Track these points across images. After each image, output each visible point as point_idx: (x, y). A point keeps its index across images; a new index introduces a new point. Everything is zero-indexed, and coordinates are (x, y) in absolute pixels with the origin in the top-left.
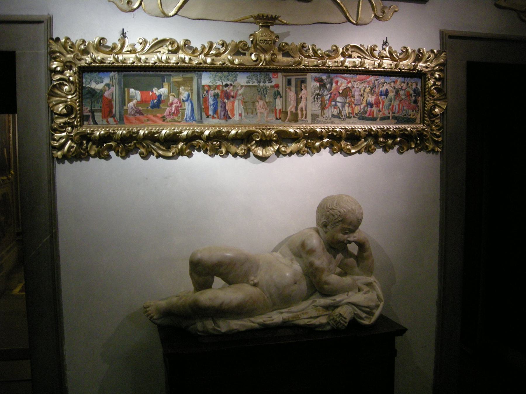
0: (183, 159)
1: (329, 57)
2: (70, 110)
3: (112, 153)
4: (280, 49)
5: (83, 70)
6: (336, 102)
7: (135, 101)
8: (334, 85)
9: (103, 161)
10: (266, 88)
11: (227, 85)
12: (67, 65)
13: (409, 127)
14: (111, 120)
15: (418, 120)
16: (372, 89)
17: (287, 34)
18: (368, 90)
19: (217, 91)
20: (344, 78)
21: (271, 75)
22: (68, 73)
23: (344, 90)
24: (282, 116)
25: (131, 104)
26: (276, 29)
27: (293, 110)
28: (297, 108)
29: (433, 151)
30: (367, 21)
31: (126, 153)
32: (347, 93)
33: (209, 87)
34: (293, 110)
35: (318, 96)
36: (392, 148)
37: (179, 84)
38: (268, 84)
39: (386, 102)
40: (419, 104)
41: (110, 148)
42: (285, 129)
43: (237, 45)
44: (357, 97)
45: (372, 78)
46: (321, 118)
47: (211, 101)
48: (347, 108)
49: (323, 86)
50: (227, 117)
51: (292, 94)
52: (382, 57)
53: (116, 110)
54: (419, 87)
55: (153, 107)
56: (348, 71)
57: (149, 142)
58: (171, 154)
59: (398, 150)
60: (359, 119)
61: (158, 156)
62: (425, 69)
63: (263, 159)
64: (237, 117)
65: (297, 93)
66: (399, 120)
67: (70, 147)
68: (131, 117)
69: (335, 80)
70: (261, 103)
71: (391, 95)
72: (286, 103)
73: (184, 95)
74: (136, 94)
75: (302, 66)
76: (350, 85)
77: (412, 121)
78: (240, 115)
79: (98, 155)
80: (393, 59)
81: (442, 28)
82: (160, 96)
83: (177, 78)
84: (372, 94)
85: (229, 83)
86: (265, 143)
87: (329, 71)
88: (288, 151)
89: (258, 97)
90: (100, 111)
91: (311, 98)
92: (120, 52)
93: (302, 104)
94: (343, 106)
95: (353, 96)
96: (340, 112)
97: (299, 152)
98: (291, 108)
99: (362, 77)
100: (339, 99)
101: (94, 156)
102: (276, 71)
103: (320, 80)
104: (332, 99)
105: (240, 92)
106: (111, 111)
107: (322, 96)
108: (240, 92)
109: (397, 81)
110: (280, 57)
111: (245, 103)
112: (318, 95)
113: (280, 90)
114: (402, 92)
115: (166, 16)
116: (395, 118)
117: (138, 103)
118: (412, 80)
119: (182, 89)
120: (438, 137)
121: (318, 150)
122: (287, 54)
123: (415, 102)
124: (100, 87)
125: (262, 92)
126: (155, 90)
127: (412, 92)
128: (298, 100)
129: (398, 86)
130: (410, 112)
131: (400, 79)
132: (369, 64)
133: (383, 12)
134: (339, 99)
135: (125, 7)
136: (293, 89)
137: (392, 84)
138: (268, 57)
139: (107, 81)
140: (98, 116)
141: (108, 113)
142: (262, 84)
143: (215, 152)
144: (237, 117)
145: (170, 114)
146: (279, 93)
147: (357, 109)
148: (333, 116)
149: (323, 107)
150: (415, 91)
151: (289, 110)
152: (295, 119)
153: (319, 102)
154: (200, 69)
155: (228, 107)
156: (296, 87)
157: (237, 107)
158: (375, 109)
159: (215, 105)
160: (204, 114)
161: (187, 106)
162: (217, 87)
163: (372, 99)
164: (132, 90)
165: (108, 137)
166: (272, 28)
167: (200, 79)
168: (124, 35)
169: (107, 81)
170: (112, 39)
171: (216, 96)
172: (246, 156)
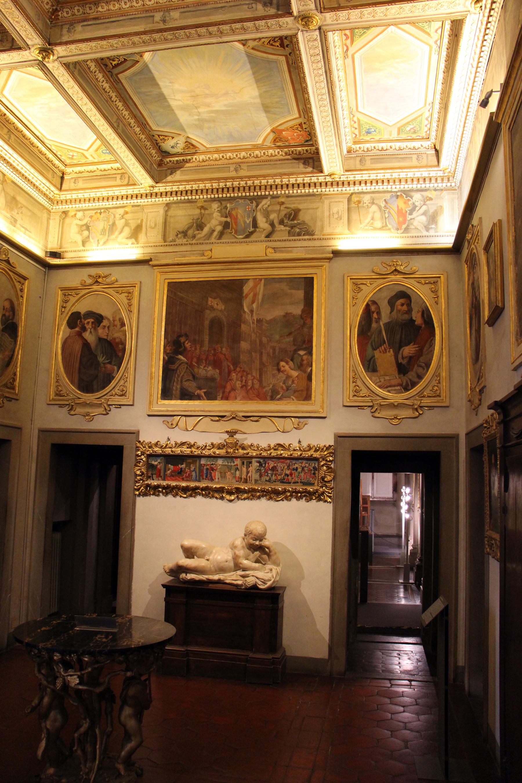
0: (192, 499)
1: (265, 450)
2: (143, 473)
3: (161, 494)
4: (240, 447)
5: (149, 456)
6: (268, 473)
7: (170, 471)
8: (267, 465)
9: (156, 497)
10: (231, 466)
11: (212, 464)
12: (143, 453)
13: (310, 489)
14: (160, 478)
15: (316, 484)
16: (288, 467)
17: (246, 439)
18: (286, 467)
19: (208, 467)
20: (272, 461)
21: (234, 460)
22: (143, 457)
23: (272, 467)
24: (239, 480)
25: (169, 472)
26: (237, 436)
27: (245, 477)
28: (247, 476)
29: (326, 501)
30: (289, 430)
31: (166, 494)
32: (274, 469)
33: (204, 464)
34: (245, 477)
35: (259, 470)
36: (302, 499)
37: (190, 463)
38: (232, 464)
39: (297, 474)
40: (317, 475)
41: (159, 491)
42: (240, 486)
43: (219, 444)
44: (279, 471)
45: (288, 461)
46: (259, 482)
47: (205, 472)
48: (274, 477)
49: (261, 465)
50: (212, 480)
51: (244, 469)
52: (294, 450)
53: (162, 474)
54: (316, 465)
55: (178, 473)
56: (274, 457)
57: (177, 490)
58: (185, 496)
59: (305, 499)
60: (281, 482)
61: (181, 496)
62: (318, 456)
63: (230, 501)
64: (217, 480)
65: (247, 469)
66: (304, 484)
67: (143, 490)
68: (169, 478)
69: (268, 462)
70: (229, 473)
71: (299, 470)
72: (241, 474)
73: (192, 468)
74: (171, 467)
75: (249, 455)
76: (275, 465)
77: (312, 484)
78: (218, 479)
79: (154, 494)
80: (302, 451)
81: (336, 431)
82: (182, 468)
83: (190, 461)
84: (288, 470)
85: (213, 463)
86: (230, 493)
87: (264, 458)
88: (243, 498)
89: (227, 470)
90: (155, 474)
91: (254, 471)
92: (166, 447)
93: (250, 474)
94: (272, 476)
95: (277, 471)
96: (270, 479)
97: (248, 498)
98: (244, 476)
99: (282, 460)
100: (269, 472)
101: (153, 494)
102: (236, 458)
103: (259, 462)
104: (266, 472)
105: (219, 468)
106: (160, 474)
107: (260, 470)
108: (219, 468)
109: (303, 462)
110: (240, 451)
111: (221, 473)
112: (258, 469)
113: (239, 467)
114: (306, 469)
115: (188, 431)
116: (301, 482)
117: (172, 471)
118: (312, 462)
119: (191, 465)
120: (329, 493)
121: (259, 498)
122: (243, 448)
123: (314, 474)
124: (156, 463)
125: (229, 468)
126: (179, 466)
127: (312, 468)
128: (248, 472)
129: (303, 465)
130: (311, 479)
131: (304, 462)
132: (286, 454)
133: (298, 425)
134: (269, 472)
135: (170, 426)
136: (245, 466)
137: (300, 464)
138: (232, 450)
139: (159, 461)
140: (154, 476)
141: (159, 476)
142: (229, 464)
143: (206, 496)
144: (217, 480)
145: (186, 477)
146: (238, 469)
147: (279, 478)
148: (266, 481)
149: (261, 476)
150: (314, 468)
151: (243, 477)
152: (246, 481)
153: (259, 473)
154: (199, 457)
155: (213, 475)
156: (247, 465)
157: (217, 475)
158: (290, 477)
159: (207, 473)
160: (201, 478)
161: (194, 474)
162: (208, 465)
163: (288, 472)
164: (170, 465)
165: (158, 486)
166: (234, 436)
167: (200, 461)
168: (169, 439)
169: (159, 461)
170: (163, 442)
171: (207, 469)
172: (222, 498)
